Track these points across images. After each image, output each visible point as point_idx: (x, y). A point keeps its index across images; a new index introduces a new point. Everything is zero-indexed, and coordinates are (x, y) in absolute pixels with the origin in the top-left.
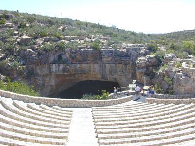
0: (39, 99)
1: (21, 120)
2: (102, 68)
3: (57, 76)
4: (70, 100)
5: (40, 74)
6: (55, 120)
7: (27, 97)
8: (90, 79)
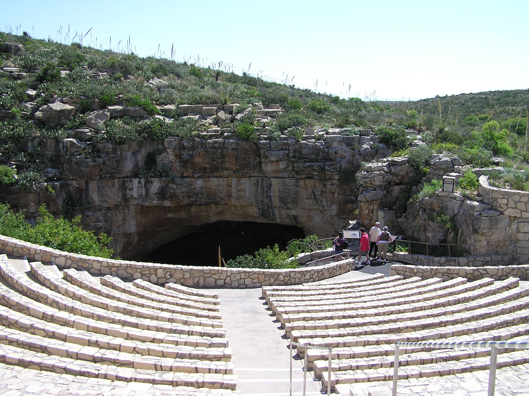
0: (127, 266)
1: (100, 318)
2: (262, 188)
3: (143, 210)
4: (205, 268)
5: (97, 203)
6: (184, 318)
7: (98, 261)
8: (228, 217)
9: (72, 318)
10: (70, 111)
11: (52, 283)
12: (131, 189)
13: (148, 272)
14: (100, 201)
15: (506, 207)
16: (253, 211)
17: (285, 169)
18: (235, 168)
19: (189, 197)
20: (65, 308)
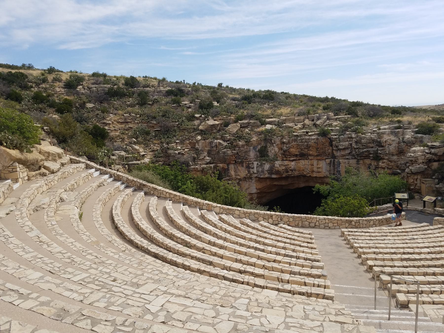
0: (255, 213)
1: (241, 245)
2: (334, 166)
3: (260, 180)
4: (302, 215)
5: (234, 176)
6: (292, 247)
7: (238, 210)
9: (226, 244)
10: (218, 125)
11: (213, 223)
12: (253, 168)
13: (267, 217)
14: (236, 175)
17: (349, 153)
18: (316, 154)
19: (287, 172)
20: (220, 238)
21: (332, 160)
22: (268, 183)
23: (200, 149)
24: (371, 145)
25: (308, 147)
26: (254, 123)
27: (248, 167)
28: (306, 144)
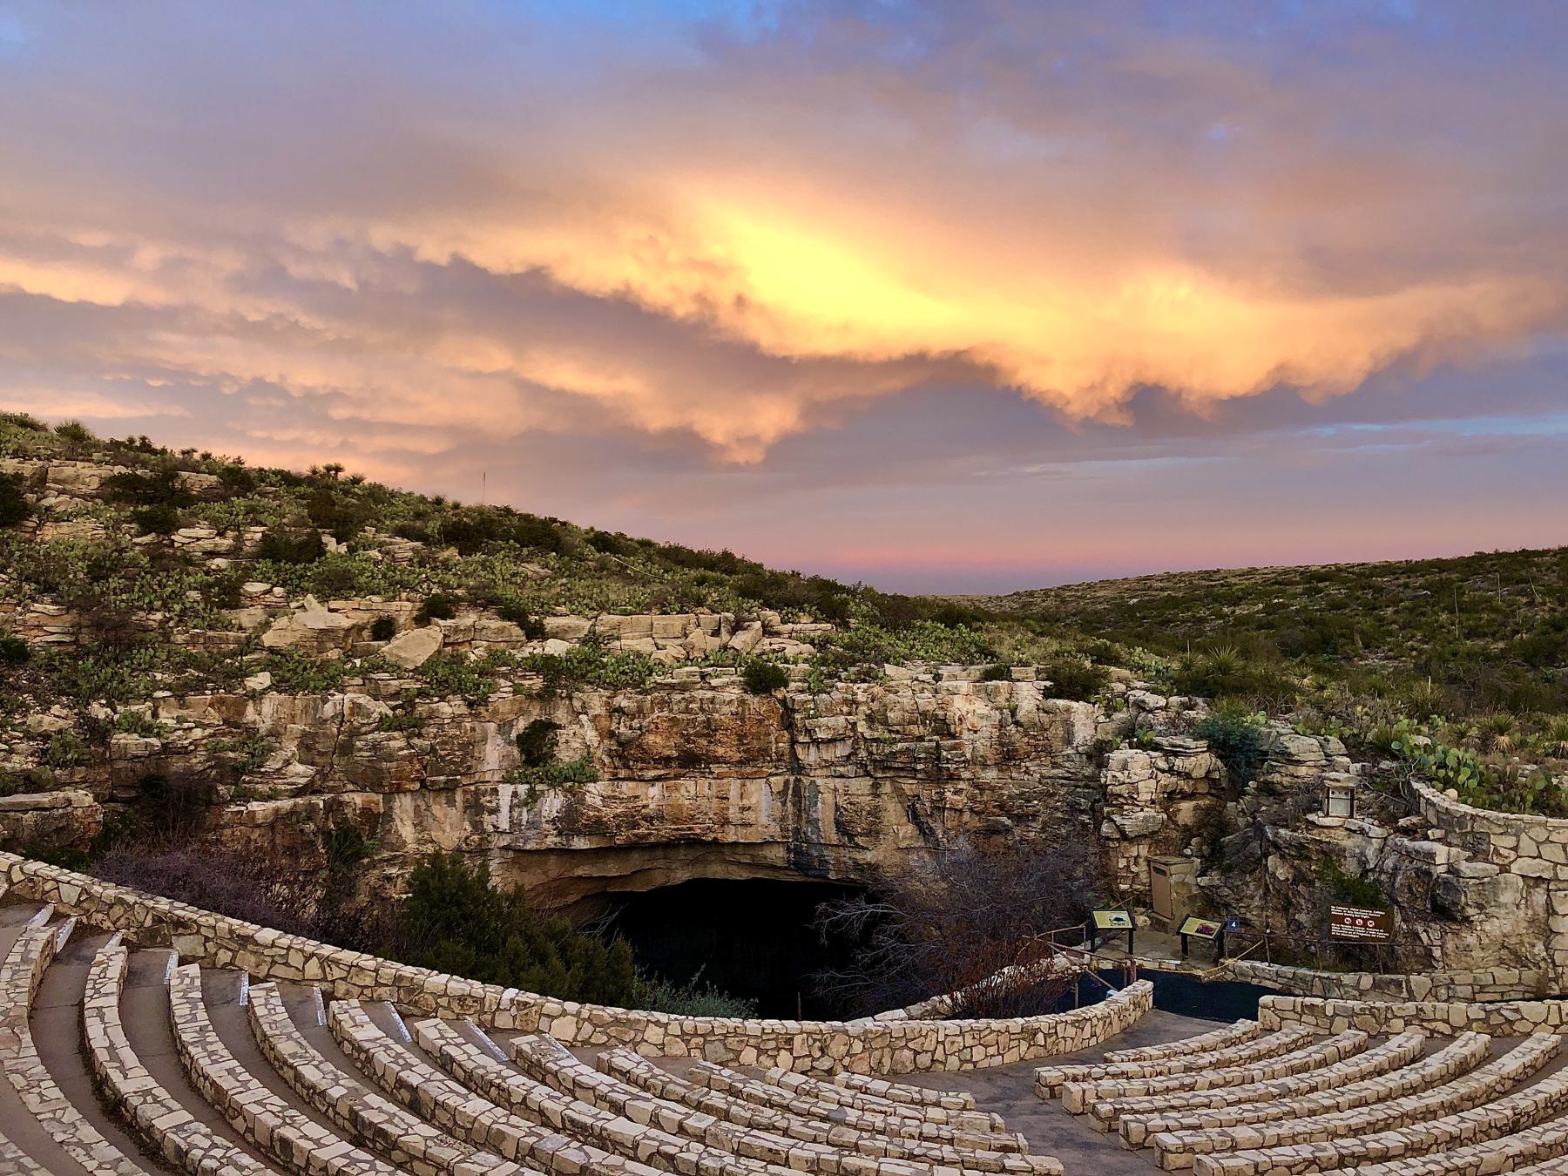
5: (411, 846)
7: (657, 1023)
12: (495, 811)
13: (772, 1044)
14: (418, 841)
15: (1513, 855)
16: (777, 855)
17: (848, 757)
19: (635, 825)
21: (792, 779)
22: (554, 868)
23: (263, 728)
24: (917, 730)
25: (710, 730)
26: (501, 630)
27: (475, 808)
28: (701, 717)
